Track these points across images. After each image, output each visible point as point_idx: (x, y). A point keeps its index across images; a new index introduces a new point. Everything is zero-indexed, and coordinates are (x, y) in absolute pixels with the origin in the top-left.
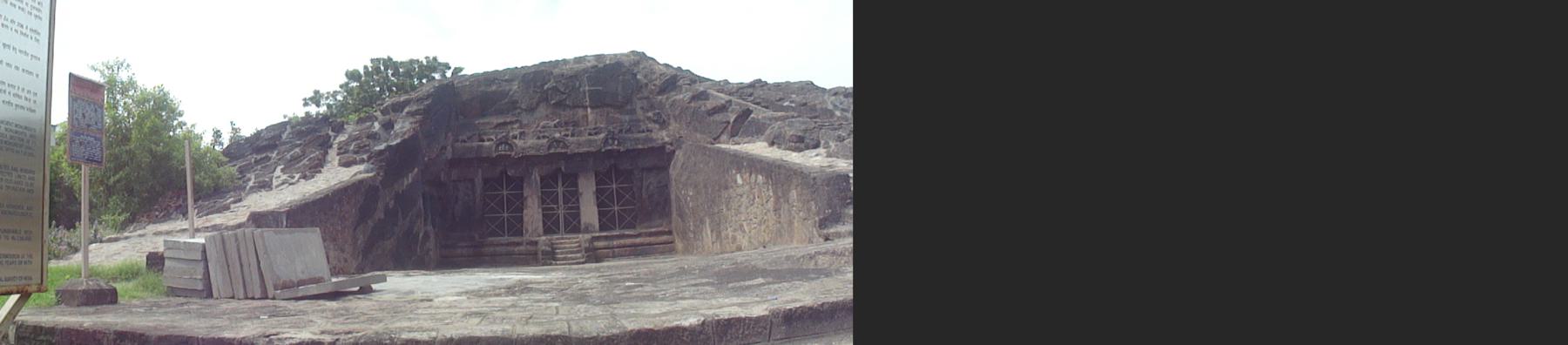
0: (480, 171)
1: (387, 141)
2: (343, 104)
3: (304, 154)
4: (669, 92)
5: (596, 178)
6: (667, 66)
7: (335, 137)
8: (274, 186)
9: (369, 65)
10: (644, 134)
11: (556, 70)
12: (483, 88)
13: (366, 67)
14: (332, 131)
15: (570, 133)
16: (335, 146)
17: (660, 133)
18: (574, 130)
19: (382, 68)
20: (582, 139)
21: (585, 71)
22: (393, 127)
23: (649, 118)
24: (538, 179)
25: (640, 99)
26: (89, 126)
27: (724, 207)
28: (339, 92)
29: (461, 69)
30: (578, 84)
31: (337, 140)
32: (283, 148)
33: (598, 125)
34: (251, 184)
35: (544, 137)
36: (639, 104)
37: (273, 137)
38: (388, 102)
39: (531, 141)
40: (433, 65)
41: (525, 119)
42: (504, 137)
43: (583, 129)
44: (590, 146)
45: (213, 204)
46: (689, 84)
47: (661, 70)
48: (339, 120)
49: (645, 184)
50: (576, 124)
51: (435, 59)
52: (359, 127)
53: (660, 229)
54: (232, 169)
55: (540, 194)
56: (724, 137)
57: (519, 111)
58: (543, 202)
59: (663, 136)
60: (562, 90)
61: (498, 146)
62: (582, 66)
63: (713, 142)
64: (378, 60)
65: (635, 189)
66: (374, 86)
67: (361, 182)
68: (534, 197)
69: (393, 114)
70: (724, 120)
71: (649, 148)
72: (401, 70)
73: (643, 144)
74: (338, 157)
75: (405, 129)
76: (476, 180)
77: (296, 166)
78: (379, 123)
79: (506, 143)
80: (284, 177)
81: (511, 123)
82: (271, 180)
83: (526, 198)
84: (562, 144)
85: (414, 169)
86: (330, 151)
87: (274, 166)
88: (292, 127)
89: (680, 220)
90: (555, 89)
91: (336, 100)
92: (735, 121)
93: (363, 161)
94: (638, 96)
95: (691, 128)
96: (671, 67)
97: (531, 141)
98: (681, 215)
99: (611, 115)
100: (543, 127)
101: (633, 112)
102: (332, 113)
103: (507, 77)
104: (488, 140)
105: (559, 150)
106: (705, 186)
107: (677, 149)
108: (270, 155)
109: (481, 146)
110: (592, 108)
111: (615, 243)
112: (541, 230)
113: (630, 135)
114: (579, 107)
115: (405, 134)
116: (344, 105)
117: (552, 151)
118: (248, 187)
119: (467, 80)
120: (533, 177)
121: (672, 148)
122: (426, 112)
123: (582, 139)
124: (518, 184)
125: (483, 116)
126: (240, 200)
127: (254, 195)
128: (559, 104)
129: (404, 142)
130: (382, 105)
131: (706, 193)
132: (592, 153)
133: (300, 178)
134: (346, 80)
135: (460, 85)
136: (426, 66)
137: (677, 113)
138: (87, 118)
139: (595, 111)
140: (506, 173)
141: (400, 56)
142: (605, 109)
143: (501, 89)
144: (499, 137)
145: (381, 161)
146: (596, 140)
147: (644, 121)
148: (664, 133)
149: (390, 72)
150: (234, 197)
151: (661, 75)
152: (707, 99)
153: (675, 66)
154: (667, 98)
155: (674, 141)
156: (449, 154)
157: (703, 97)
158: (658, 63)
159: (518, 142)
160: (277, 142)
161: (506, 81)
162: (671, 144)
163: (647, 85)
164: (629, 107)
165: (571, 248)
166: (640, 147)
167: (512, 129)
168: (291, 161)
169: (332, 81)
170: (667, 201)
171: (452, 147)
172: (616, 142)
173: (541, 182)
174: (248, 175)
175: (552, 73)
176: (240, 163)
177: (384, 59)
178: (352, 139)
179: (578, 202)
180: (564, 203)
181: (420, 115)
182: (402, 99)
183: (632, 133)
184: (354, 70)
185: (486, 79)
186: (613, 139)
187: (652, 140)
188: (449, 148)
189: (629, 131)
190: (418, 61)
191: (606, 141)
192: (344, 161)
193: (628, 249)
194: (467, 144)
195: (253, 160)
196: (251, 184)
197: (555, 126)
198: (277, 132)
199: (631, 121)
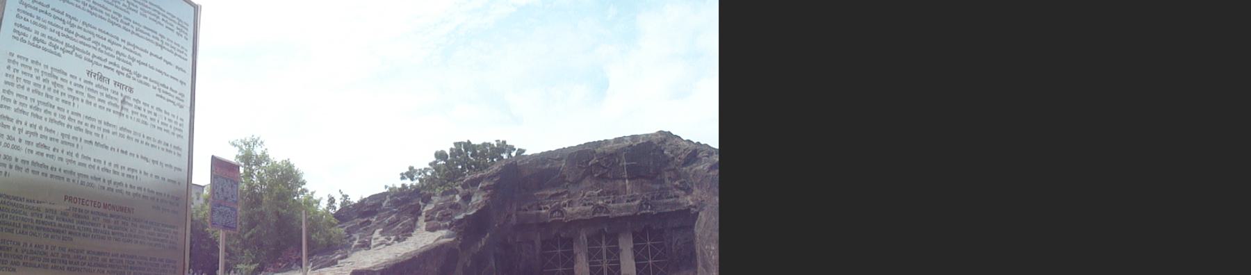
1: (465, 211)
2: (431, 179)
3: (398, 221)
4: (692, 164)
5: (633, 237)
7: (425, 206)
8: (372, 246)
9: (453, 147)
10: (671, 200)
11: (599, 149)
12: (539, 166)
13: (451, 149)
14: (422, 201)
15: (610, 200)
16: (424, 214)
17: (686, 198)
18: (614, 198)
19: (463, 149)
20: (621, 205)
21: (623, 149)
22: (470, 200)
23: (676, 186)
25: (668, 171)
26: (226, 199)
28: (429, 169)
29: (524, 151)
30: (617, 160)
31: (426, 209)
32: (382, 214)
33: (634, 193)
34: (356, 243)
35: (589, 204)
36: (667, 175)
37: (374, 205)
38: (468, 178)
39: (578, 208)
40: (503, 147)
41: (572, 190)
42: (556, 205)
43: (622, 196)
44: (628, 211)
45: (325, 259)
47: (685, 146)
48: (427, 192)
50: (616, 193)
51: (504, 142)
52: (443, 199)
54: (341, 230)
55: (587, 251)
57: (567, 183)
58: (590, 257)
59: (688, 200)
60: (604, 165)
61: (552, 213)
62: (621, 145)
64: (460, 143)
66: (457, 165)
67: (443, 246)
69: (471, 188)
71: (676, 211)
72: (478, 151)
73: (671, 208)
74: (425, 224)
75: (479, 202)
77: (393, 230)
78: (460, 196)
79: (559, 211)
80: (382, 239)
81: (562, 194)
82: (371, 241)
83: (576, 255)
84: (605, 209)
85: (486, 234)
86: (419, 218)
87: (373, 229)
88: (391, 197)
89: (704, 270)
90: (598, 165)
91: (426, 175)
93: (445, 227)
94: (665, 169)
97: (578, 208)
99: (644, 184)
100: (589, 196)
101: (662, 181)
102: (423, 185)
103: (558, 157)
104: (545, 209)
105: (603, 215)
107: (700, 211)
108: (371, 220)
109: (539, 214)
110: (629, 179)
113: (661, 201)
114: (619, 179)
115: (479, 205)
116: (432, 180)
117: (596, 215)
118: (353, 246)
119: (527, 160)
120: (581, 238)
121: (695, 210)
122: (496, 187)
123: (621, 205)
124: (569, 243)
125: (540, 189)
126: (346, 257)
127: (358, 253)
128: (602, 177)
129: (479, 212)
130: (462, 180)
132: (630, 216)
133: (394, 240)
134: (435, 159)
135: (522, 164)
136: (496, 148)
137: (699, 180)
138: (225, 194)
139: (631, 182)
141: (477, 141)
142: (639, 180)
144: (553, 206)
145: (460, 228)
146: (633, 206)
147: (671, 189)
148: (689, 198)
149: (470, 153)
150: (342, 253)
151: (685, 150)
155: (697, 205)
156: (514, 220)
159: (568, 210)
160: (377, 209)
161: (558, 159)
162: (695, 207)
163: (673, 158)
164: (659, 177)
166: (668, 210)
167: (563, 198)
168: (388, 225)
169: (423, 160)
170: (693, 254)
171: (516, 215)
172: (649, 207)
173: (588, 241)
174: (354, 235)
175: (595, 152)
176: (348, 225)
177: (464, 143)
178: (437, 208)
179: (619, 256)
180: (607, 258)
181: (490, 189)
182: (478, 175)
183: (663, 198)
184: (442, 151)
186: (647, 204)
188: (514, 215)
189: (660, 197)
190: (489, 144)
192: (429, 227)
194: (528, 212)
195: (358, 223)
196: (356, 243)
197: (599, 195)
198: (378, 201)
199: (661, 189)
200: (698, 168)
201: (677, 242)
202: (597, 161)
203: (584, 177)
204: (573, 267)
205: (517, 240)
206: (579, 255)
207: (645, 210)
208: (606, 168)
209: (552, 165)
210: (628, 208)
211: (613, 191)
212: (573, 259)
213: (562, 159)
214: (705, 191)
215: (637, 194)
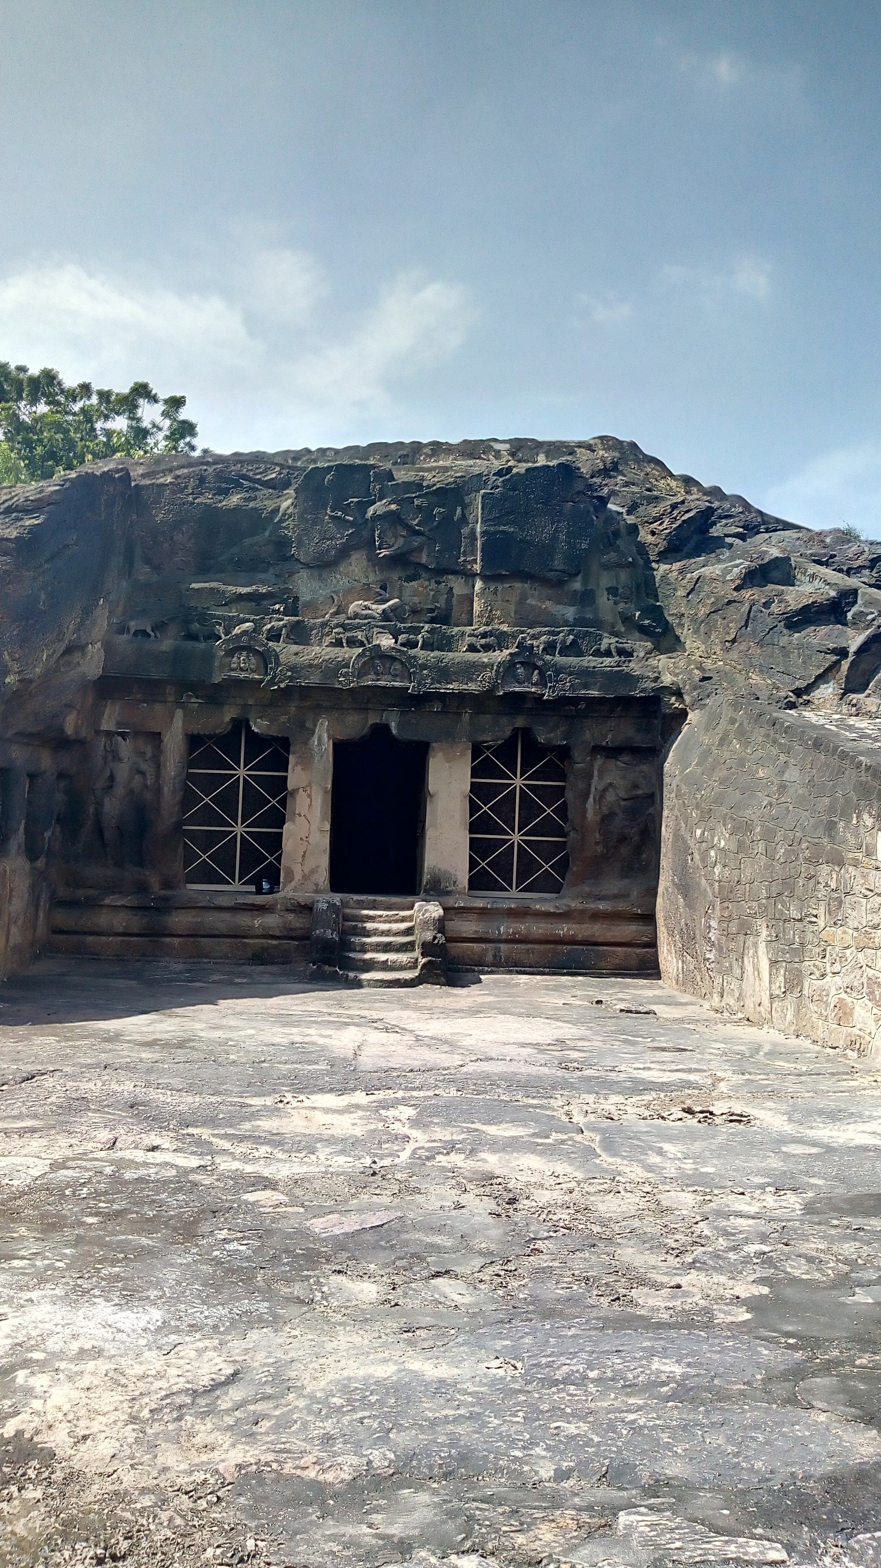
0: (179, 714)
4: (689, 556)
6: (688, 481)
10: (608, 661)
12: (206, 498)
17: (653, 662)
24: (328, 746)
25: (606, 567)
27: (821, 911)
42: (245, 633)
43: (456, 629)
44: (471, 680)
46: (741, 537)
49: (596, 784)
50: (443, 618)
53: (622, 906)
56: (827, 691)
63: (793, 699)
65: (569, 795)
70: (832, 646)
76: (167, 738)
79: (249, 649)
92: (863, 649)
95: (734, 655)
96: (697, 484)
98: (686, 888)
101: (586, 598)
106: (768, 836)
110: (485, 578)
111: (505, 928)
114: (454, 573)
128: (399, 560)
131: (769, 854)
137: (703, 611)
140: (249, 727)
142: (518, 585)
143: (252, 504)
146: (485, 666)
148: (662, 661)
151: (674, 507)
152: (789, 580)
153: (706, 483)
154: (681, 571)
157: (776, 574)
158: (672, 475)
161: (270, 484)
164: (577, 585)
165: (387, 933)
166: (594, 693)
172: (535, 678)
183: (580, 654)
185: (220, 476)
187: (630, 679)
189: (572, 649)
191: (508, 669)
193: (535, 946)
199: (580, 621)
200: (706, 571)
201: (605, 790)
202: (393, 507)
203: (344, 553)
205: (104, 727)
206: (301, 790)
207: (520, 683)
208: (419, 533)
209: (250, 499)
210: (469, 671)
211: (432, 610)
212: (283, 803)
213: (286, 484)
214: (718, 649)
215: (505, 628)
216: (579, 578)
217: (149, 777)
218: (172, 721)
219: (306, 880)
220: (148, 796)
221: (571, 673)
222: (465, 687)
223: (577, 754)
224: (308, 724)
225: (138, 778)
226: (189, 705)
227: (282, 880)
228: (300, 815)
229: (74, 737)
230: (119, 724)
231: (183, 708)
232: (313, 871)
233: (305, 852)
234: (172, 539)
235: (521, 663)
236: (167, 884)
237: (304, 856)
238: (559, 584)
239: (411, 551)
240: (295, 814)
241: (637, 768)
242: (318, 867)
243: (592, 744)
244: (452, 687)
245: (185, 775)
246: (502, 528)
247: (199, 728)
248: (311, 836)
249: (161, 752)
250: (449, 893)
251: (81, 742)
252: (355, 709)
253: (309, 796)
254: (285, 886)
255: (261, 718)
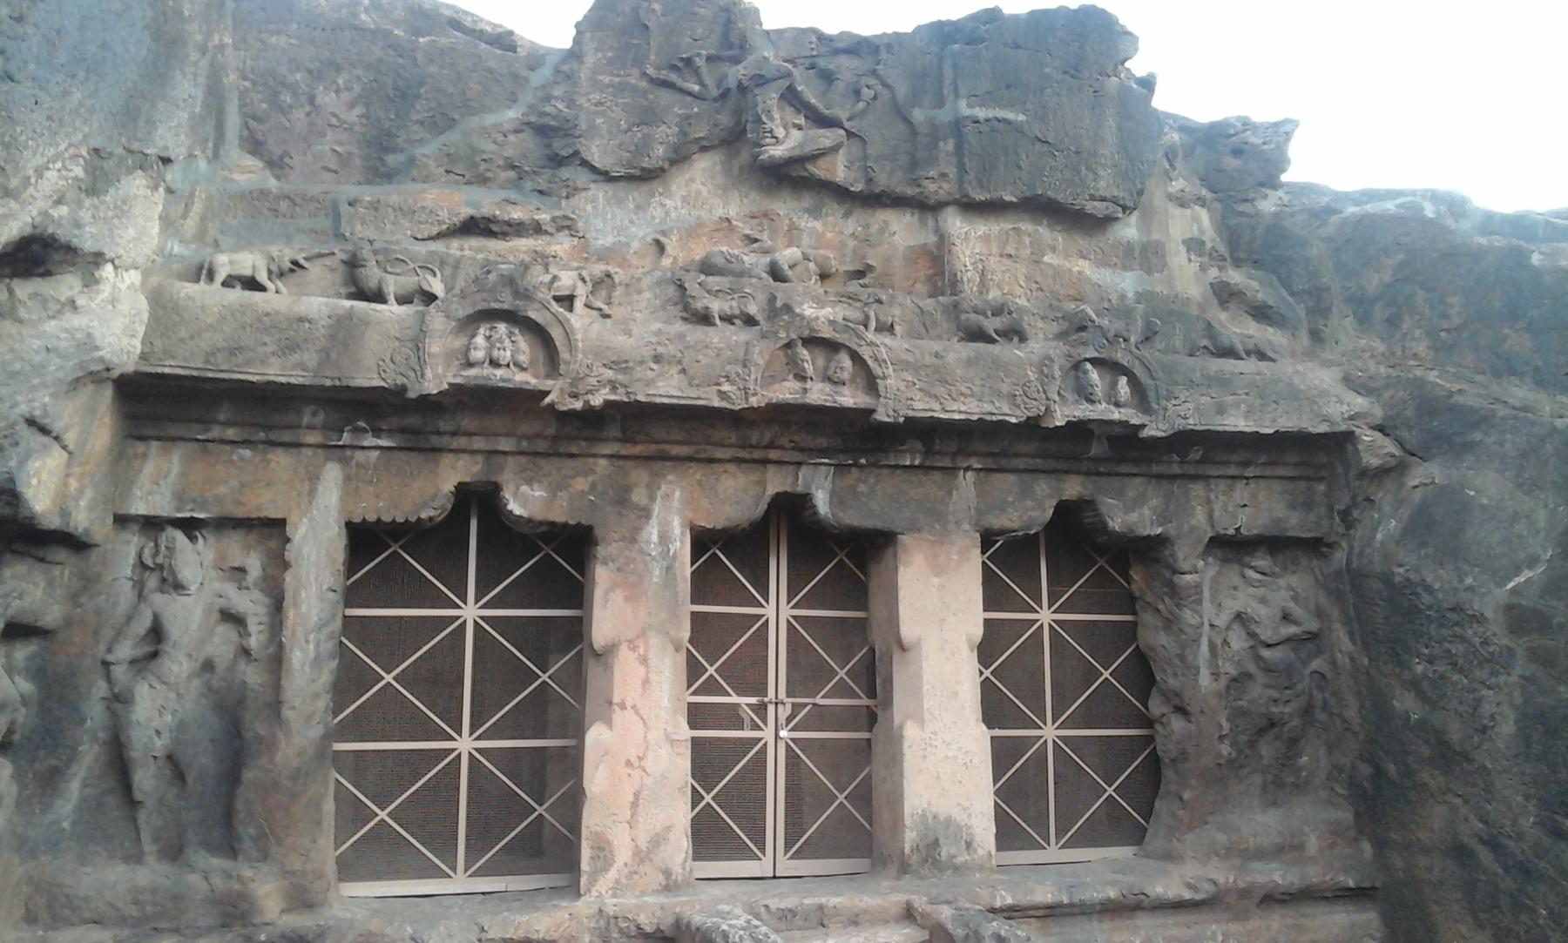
24: (682, 546)
58: (694, 670)
68: (655, 641)
76: (299, 531)
79: (511, 317)
83: (611, 649)
105: (818, 394)
112: (680, 844)
114: (898, 202)
117: (786, 391)
120: (652, 533)
142: (1026, 226)
164: (1129, 230)
173: (695, 556)
194: (277, 300)
203: (679, 157)
204: (579, 733)
205: (140, 508)
206: (624, 652)
212: (576, 679)
214: (1421, 348)
216: (1134, 218)
217: (253, 627)
218: (312, 493)
219: (642, 861)
220: (253, 676)
221: (1191, 385)
222: (988, 407)
223: (1186, 555)
224: (639, 496)
225: (226, 632)
226: (359, 455)
227: (585, 866)
228: (623, 706)
229: (54, 523)
230: (180, 498)
231: (344, 461)
232: (657, 841)
233: (637, 795)
234: (312, 100)
235: (1093, 361)
236: (301, 899)
237: (635, 804)
238: (1100, 224)
239: (813, 158)
240: (610, 703)
241: (1282, 582)
242: (668, 829)
243: (1210, 534)
244: (963, 408)
245: (338, 623)
246: (1001, 114)
247: (376, 507)
248: (650, 755)
249: (286, 566)
250: (957, 869)
251: (76, 544)
252: (739, 461)
253: (644, 661)
254: (592, 882)
255: (529, 482)
